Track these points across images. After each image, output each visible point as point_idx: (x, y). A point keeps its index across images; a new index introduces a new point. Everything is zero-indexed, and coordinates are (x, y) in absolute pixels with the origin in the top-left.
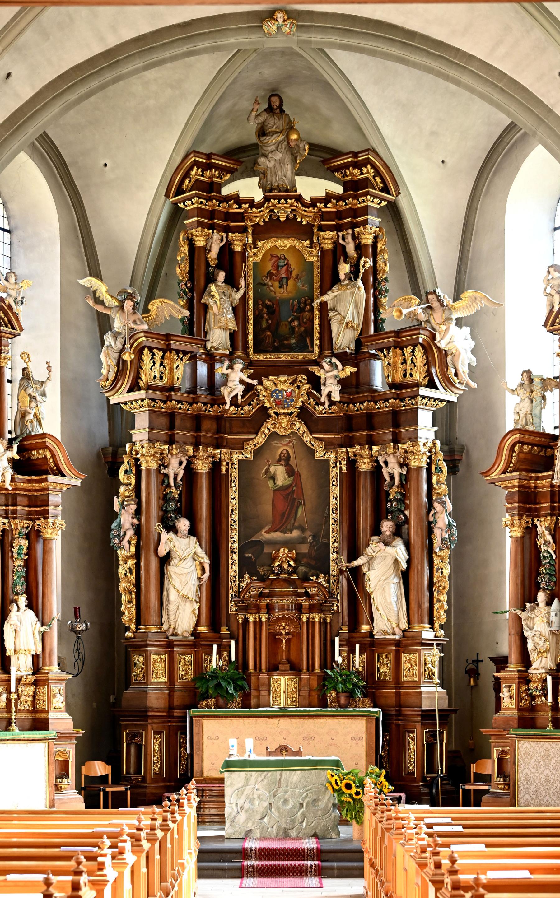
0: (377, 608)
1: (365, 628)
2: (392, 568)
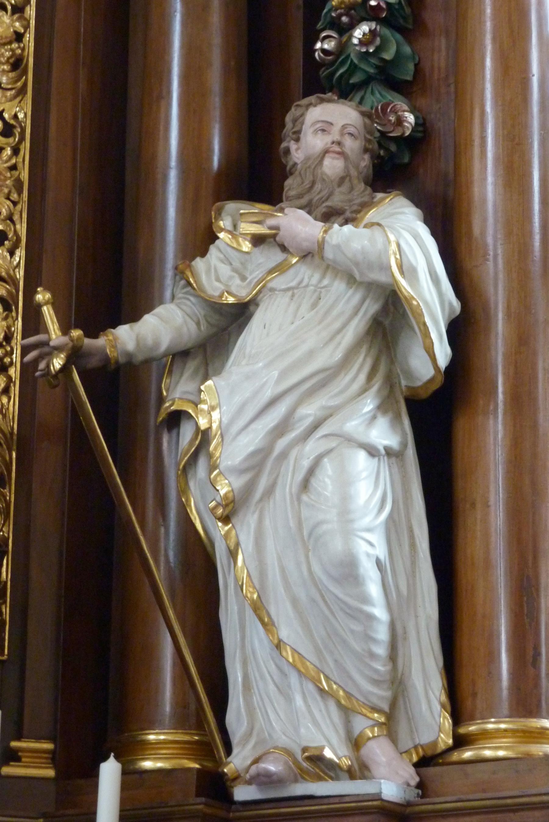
0: (258, 608)
1: (162, 751)
2: (362, 364)
